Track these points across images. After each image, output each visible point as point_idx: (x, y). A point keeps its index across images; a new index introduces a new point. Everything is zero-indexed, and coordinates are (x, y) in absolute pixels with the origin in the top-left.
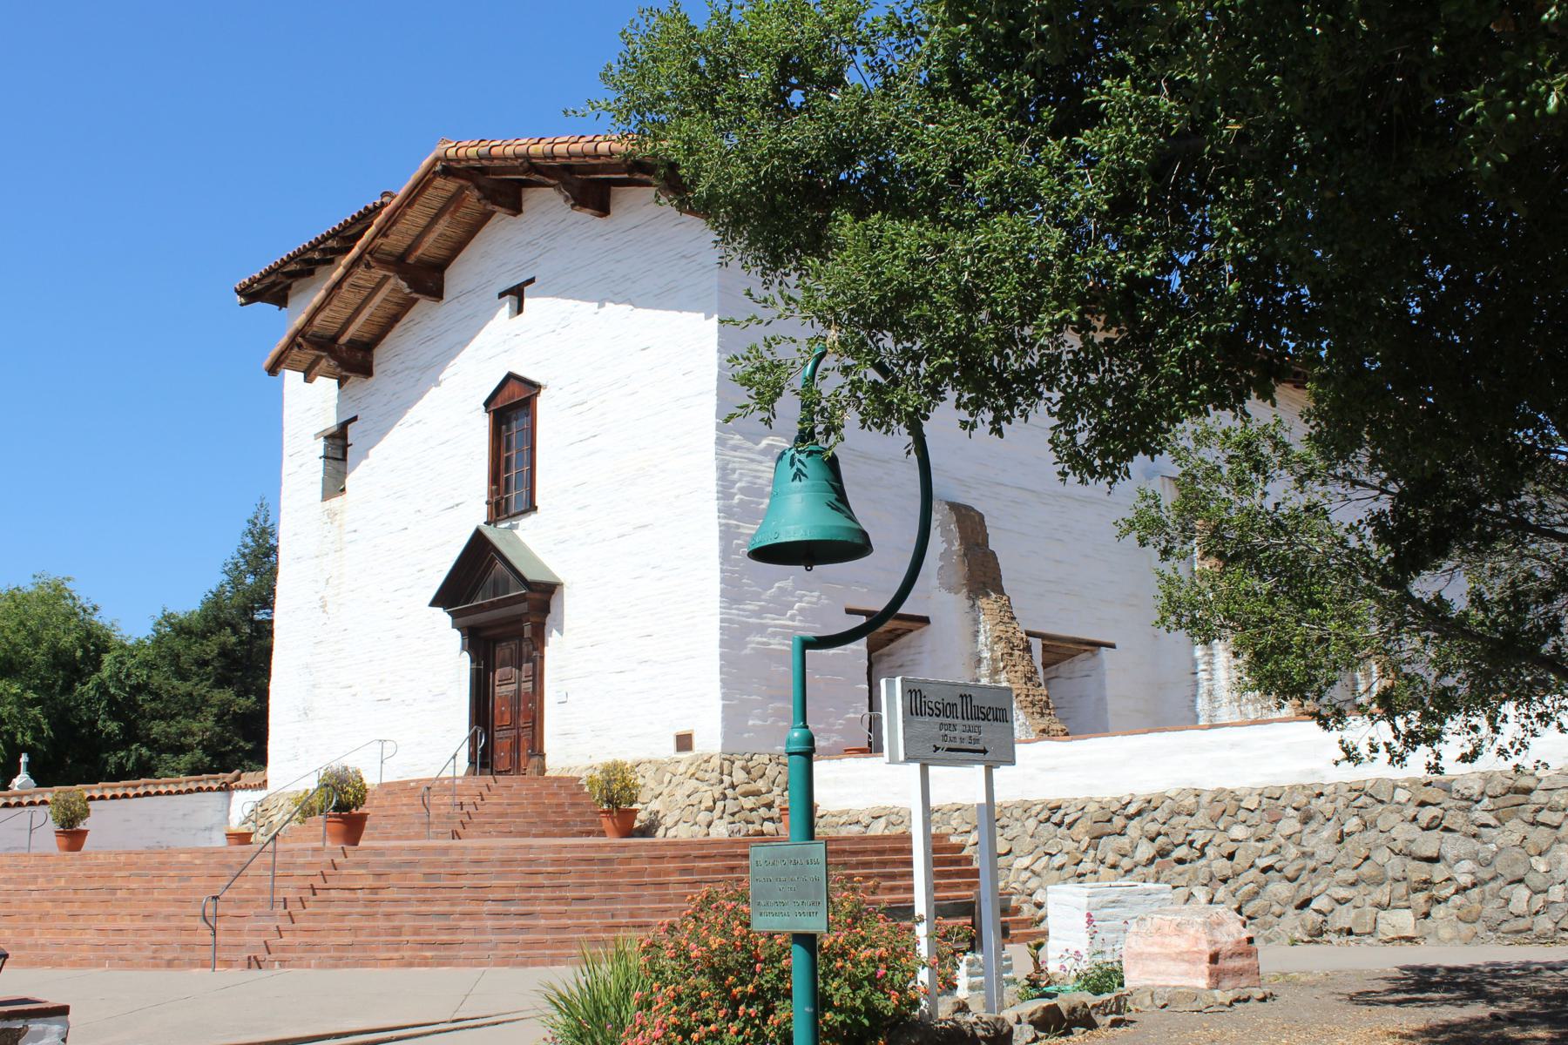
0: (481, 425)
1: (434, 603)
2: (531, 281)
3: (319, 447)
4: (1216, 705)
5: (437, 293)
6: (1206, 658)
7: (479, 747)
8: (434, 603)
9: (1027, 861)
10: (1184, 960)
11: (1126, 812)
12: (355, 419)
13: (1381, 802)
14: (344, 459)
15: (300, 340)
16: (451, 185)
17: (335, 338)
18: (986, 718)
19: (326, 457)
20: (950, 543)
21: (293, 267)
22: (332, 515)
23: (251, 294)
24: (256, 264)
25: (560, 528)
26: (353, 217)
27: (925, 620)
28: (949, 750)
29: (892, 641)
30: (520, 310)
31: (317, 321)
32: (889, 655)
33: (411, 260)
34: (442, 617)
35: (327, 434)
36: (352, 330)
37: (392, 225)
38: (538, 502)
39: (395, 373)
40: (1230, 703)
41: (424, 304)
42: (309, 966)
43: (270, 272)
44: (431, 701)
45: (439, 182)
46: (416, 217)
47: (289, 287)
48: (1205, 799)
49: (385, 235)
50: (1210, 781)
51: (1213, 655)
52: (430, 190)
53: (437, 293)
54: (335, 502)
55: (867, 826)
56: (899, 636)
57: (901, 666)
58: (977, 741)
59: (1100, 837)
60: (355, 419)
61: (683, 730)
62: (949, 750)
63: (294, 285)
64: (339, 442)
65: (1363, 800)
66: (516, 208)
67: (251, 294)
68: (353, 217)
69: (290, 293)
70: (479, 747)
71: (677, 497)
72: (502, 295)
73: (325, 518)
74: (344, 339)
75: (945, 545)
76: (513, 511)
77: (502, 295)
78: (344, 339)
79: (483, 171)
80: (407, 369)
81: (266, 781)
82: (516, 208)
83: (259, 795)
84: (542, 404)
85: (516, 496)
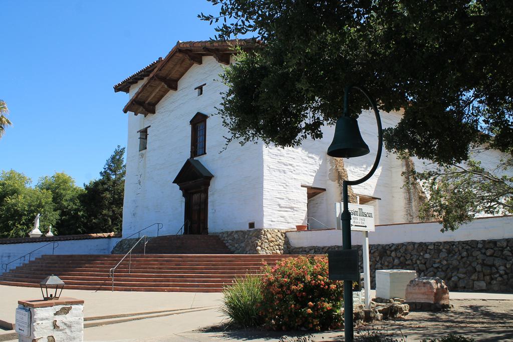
0: (189, 129)
2: (205, 84)
3: (139, 135)
5: (175, 88)
7: (189, 226)
10: (426, 294)
11: (391, 249)
12: (150, 126)
13: (473, 248)
14: (146, 138)
15: (134, 102)
16: (181, 55)
17: (144, 102)
18: (366, 216)
19: (140, 138)
21: (131, 80)
22: (142, 155)
23: (118, 89)
24: (119, 80)
26: (150, 65)
27: (324, 190)
28: (355, 226)
29: (314, 196)
30: (201, 93)
31: (139, 96)
32: (313, 200)
33: (168, 78)
34: (177, 187)
36: (149, 99)
37: (163, 67)
38: (206, 152)
39: (162, 112)
41: (171, 92)
43: (124, 82)
45: (177, 54)
46: (170, 65)
47: (130, 87)
49: (160, 70)
52: (174, 57)
53: (175, 88)
54: (143, 151)
56: (317, 194)
57: (317, 204)
58: (364, 223)
60: (150, 126)
61: (251, 222)
62: (355, 226)
63: (131, 86)
64: (145, 133)
65: (467, 247)
66: (200, 62)
67: (118, 89)
68: (150, 65)
69: (130, 88)
70: (189, 226)
72: (195, 89)
74: (146, 102)
75: (331, 167)
76: (198, 155)
77: (195, 89)
78: (146, 102)
79: (191, 51)
80: (166, 111)
82: (200, 62)
83: (120, 240)
84: (208, 121)
85: (200, 151)
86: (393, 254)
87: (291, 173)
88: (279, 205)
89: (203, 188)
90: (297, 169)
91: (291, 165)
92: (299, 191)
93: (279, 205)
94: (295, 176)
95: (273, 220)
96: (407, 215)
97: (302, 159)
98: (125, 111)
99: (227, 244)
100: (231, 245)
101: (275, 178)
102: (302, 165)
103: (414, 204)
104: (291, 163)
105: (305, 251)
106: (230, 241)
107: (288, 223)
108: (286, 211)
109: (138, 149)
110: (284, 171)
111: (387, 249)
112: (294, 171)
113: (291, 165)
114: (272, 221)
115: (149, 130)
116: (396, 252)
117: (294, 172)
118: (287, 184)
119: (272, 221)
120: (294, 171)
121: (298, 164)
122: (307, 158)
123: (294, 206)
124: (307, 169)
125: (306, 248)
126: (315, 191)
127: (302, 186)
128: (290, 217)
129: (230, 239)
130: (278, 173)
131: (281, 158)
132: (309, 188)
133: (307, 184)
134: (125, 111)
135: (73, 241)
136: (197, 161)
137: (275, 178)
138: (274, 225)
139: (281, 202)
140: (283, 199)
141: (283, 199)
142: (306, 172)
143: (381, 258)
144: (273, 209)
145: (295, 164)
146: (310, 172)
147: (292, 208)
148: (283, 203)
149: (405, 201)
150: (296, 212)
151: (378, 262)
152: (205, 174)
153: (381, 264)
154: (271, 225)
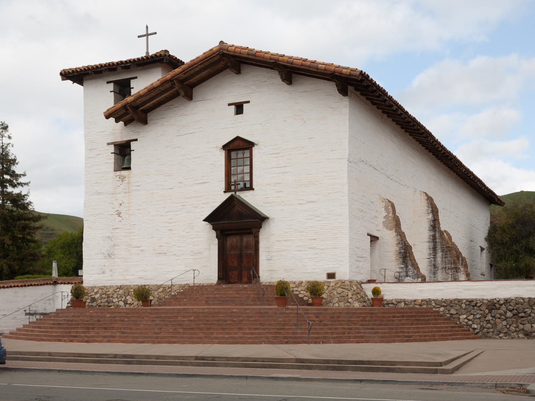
1: (205, 220)
3: (112, 148)
4: (437, 269)
6: (434, 254)
8: (205, 220)
9: (465, 316)
20: (389, 213)
25: (266, 198)
35: (115, 144)
40: (442, 269)
42: (331, 343)
44: (191, 255)
48: (527, 300)
50: (526, 295)
51: (436, 253)
53: (190, 97)
54: (124, 173)
55: (396, 305)
59: (492, 310)
61: (331, 271)
71: (329, 193)
72: (229, 105)
73: (118, 179)
81: (83, 281)
84: (255, 150)
86: (504, 308)
89: (254, 230)
96: (431, 266)
99: (300, 296)
100: (305, 296)
103: (439, 254)
105: (393, 304)
106: (302, 292)
109: (112, 167)
111: (496, 303)
115: (133, 145)
116: (505, 305)
125: (392, 300)
129: (302, 290)
135: (16, 289)
136: (239, 196)
143: (490, 312)
149: (429, 251)
151: (487, 314)
152: (264, 216)
153: (492, 316)
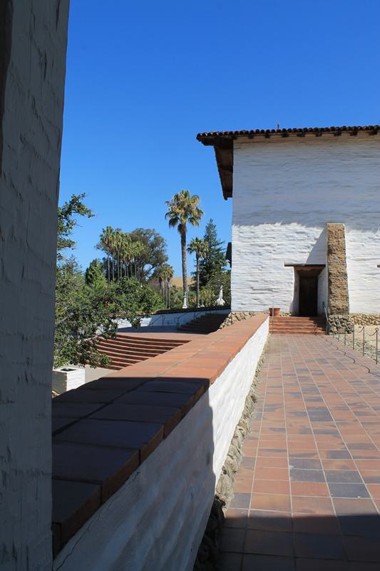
87: (269, 254)
88: (252, 288)
90: (278, 249)
91: (269, 245)
92: (280, 271)
93: (252, 288)
94: (276, 257)
95: (244, 303)
97: (287, 237)
98: (226, 199)
101: (247, 262)
102: (284, 242)
104: (268, 243)
107: (264, 305)
108: (262, 293)
110: (259, 253)
112: (274, 250)
113: (269, 245)
114: (242, 304)
117: (274, 252)
118: (264, 266)
119: (242, 304)
120: (274, 250)
121: (279, 243)
122: (296, 235)
123: (272, 287)
124: (292, 246)
126: (311, 268)
127: (285, 266)
128: (266, 299)
130: (252, 256)
131: (255, 240)
132: (295, 266)
133: (294, 263)
134: (226, 199)
137: (247, 262)
138: (245, 308)
139: (252, 284)
140: (257, 281)
141: (257, 281)
142: (293, 250)
144: (244, 293)
145: (274, 243)
146: (300, 249)
147: (270, 290)
148: (256, 285)
150: (275, 294)
154: (240, 308)
